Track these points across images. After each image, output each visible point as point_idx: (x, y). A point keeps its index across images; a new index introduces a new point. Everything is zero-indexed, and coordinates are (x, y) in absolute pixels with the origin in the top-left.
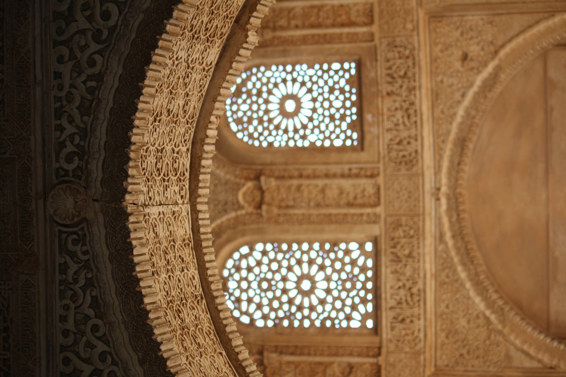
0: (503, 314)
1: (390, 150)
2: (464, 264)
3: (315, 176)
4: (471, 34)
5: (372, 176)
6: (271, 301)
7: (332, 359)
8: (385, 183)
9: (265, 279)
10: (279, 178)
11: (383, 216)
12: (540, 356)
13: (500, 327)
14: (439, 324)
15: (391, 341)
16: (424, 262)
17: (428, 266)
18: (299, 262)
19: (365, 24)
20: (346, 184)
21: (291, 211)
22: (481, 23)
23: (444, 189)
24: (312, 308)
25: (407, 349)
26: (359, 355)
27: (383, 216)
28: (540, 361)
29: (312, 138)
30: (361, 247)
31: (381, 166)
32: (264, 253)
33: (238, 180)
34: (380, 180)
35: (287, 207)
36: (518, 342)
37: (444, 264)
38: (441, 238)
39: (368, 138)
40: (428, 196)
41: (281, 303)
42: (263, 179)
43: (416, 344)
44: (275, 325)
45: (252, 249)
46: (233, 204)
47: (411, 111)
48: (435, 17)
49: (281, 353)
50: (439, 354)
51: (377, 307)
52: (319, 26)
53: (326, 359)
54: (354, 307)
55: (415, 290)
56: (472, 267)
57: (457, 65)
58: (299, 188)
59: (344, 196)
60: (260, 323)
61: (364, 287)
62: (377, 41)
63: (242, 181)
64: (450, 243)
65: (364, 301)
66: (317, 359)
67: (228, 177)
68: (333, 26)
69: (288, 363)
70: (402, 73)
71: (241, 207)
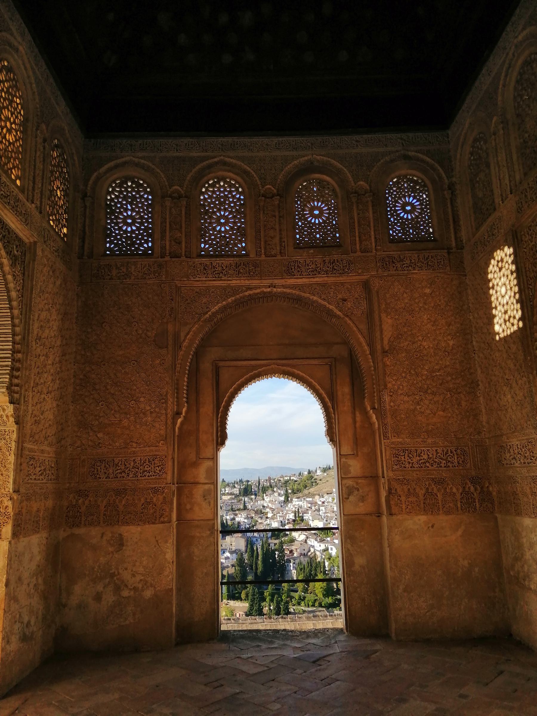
0: (209, 321)
1: (295, 262)
2: (235, 300)
3: (280, 224)
4: (357, 303)
5: (281, 253)
6: (214, 203)
7: (184, 234)
8: (278, 260)
9: (225, 201)
10: (279, 204)
11: (260, 259)
12: (187, 341)
13: (202, 319)
14: (204, 288)
15: (194, 263)
16: (236, 280)
17: (234, 282)
18: (234, 217)
19: (360, 249)
20: (277, 240)
21: (262, 212)
22: (363, 308)
23: (275, 289)
24: (211, 224)
25: (189, 272)
26: (186, 247)
27: (260, 259)
28: (184, 340)
29: (300, 224)
30: (244, 248)
31: (286, 257)
32: (239, 199)
33: (277, 185)
34: (279, 257)
35: (264, 211)
36: (194, 328)
37: (235, 290)
38: (249, 288)
39: (301, 251)
40: (270, 281)
41: (213, 208)
42: (278, 197)
43: (192, 276)
44: (201, 204)
45: (240, 193)
46: (265, 183)
47: (315, 272)
48: (366, 285)
49: (186, 207)
50: (188, 288)
51: (212, 256)
52: (359, 225)
53: (183, 229)
54: (211, 245)
55: (221, 275)
56: (234, 305)
57: (340, 296)
58: (275, 216)
59: (270, 239)
60: (202, 197)
61: (222, 250)
62: (352, 255)
63: (277, 188)
64: (247, 293)
65: (215, 250)
66: (183, 225)
67: (279, 180)
68: (359, 233)
69: (181, 211)
70: (335, 268)
71: (263, 187)
